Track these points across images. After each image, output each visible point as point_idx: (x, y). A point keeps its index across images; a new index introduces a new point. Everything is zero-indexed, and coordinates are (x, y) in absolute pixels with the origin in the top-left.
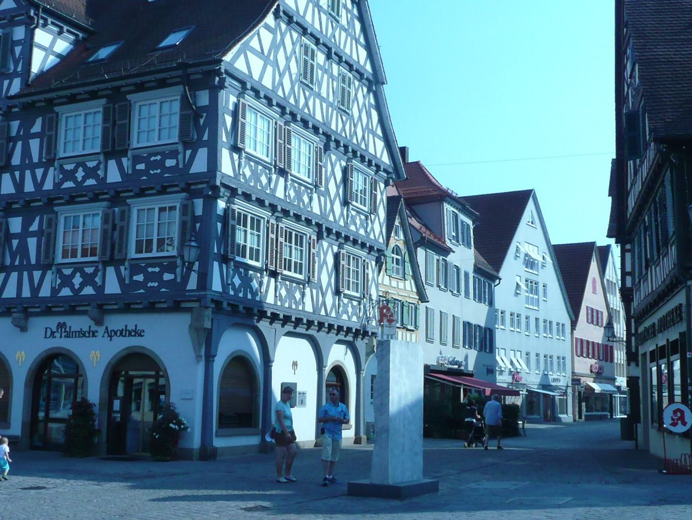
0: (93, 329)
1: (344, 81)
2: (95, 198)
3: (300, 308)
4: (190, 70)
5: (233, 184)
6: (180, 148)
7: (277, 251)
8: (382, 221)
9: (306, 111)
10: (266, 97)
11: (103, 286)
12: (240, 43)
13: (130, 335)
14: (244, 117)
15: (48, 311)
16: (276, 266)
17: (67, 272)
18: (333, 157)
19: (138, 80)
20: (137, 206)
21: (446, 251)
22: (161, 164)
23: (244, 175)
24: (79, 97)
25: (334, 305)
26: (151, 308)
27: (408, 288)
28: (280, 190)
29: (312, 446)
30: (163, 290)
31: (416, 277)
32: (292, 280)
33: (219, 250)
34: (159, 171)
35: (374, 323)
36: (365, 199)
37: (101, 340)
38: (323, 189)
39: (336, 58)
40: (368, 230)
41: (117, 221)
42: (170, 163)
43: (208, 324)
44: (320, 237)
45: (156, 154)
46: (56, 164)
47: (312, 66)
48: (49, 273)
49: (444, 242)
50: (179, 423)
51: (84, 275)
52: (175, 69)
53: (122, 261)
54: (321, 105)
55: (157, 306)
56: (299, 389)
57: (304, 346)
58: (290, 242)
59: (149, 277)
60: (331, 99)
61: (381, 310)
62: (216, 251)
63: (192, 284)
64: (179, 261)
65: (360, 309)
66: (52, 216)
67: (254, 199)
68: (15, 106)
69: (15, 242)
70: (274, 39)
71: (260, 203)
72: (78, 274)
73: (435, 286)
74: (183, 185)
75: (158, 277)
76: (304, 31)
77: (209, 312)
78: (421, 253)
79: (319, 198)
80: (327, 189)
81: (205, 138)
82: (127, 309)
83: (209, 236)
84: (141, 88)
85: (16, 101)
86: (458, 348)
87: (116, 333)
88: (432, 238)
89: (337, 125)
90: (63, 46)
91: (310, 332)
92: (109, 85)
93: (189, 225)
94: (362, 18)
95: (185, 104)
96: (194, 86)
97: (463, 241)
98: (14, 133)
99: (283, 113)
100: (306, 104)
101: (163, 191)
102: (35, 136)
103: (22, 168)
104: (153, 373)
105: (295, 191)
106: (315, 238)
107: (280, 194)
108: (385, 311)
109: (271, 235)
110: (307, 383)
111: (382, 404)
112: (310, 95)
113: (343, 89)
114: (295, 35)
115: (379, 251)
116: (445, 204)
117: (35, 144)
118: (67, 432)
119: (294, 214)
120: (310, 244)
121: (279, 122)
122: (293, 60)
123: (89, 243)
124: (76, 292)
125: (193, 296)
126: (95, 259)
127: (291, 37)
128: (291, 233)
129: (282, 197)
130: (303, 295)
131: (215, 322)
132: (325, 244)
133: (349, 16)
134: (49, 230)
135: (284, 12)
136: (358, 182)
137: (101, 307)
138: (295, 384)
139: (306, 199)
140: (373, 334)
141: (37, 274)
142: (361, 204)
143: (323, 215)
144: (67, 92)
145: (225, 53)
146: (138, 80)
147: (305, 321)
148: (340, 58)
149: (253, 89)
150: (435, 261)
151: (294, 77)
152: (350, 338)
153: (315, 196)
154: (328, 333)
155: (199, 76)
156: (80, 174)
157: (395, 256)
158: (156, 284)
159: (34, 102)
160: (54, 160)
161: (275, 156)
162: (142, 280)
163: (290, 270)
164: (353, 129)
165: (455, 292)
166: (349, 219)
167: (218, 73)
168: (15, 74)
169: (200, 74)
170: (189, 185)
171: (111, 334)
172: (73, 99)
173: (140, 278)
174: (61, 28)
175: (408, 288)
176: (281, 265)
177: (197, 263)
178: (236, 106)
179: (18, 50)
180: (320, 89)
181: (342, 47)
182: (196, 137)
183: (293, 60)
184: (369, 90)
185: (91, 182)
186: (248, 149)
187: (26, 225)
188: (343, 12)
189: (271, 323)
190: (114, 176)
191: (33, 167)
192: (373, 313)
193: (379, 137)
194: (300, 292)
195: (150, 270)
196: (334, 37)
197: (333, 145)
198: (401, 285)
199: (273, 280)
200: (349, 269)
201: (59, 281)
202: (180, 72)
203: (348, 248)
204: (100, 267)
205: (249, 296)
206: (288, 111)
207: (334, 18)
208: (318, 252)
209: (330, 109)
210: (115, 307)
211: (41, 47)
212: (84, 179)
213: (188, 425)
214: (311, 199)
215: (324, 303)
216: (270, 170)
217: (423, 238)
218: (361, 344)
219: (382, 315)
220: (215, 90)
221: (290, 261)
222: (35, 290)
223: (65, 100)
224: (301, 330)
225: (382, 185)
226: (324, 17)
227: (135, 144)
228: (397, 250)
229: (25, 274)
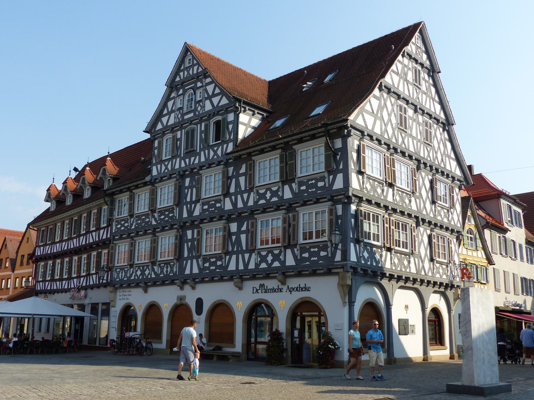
0: (281, 287)
1: (427, 125)
2: (278, 209)
3: (408, 270)
4: (329, 128)
5: (360, 194)
6: (326, 174)
7: (390, 235)
8: (458, 212)
9: (403, 146)
10: (377, 140)
11: (285, 261)
12: (359, 108)
13: (302, 290)
14: (364, 153)
15: (254, 277)
16: (390, 244)
17: (264, 253)
18: (423, 174)
19: (298, 136)
21: (505, 231)
22: (315, 185)
23: (366, 188)
24: (265, 150)
25: (430, 268)
26: (314, 273)
27: (480, 255)
28: (390, 196)
29: (421, 360)
30: (321, 262)
31: (485, 248)
32: (401, 253)
33: (353, 235)
34: (314, 190)
35: (458, 279)
36: (446, 199)
37: (285, 294)
38: (418, 194)
39: (421, 112)
40: (450, 219)
41: (291, 221)
42: (320, 184)
43: (349, 282)
44: (418, 225)
45: (312, 180)
46: (254, 190)
47: (405, 118)
48: (253, 254)
49: (503, 225)
50: (334, 344)
51: (273, 255)
52: (320, 127)
53: (295, 246)
54: (413, 142)
55: (318, 272)
56: (410, 323)
57: (412, 294)
58: (399, 229)
59: (312, 254)
60: (419, 137)
61: (462, 270)
62: (351, 236)
63: (338, 257)
64: (329, 244)
65: (448, 270)
66: (254, 221)
67: (373, 203)
68: (230, 159)
69: (234, 238)
70: (380, 104)
71: (378, 205)
72: (270, 255)
73: (499, 254)
74: (329, 197)
75: (317, 254)
76: (399, 97)
77: (349, 275)
78: (487, 232)
79: (415, 199)
80: (421, 194)
81: (341, 167)
82: (300, 274)
83: (347, 227)
84: (301, 141)
85: (231, 156)
86: (518, 295)
87: (293, 289)
88: (494, 222)
89: (424, 154)
90: (255, 122)
91: (415, 286)
92: (282, 141)
93: (334, 221)
94: (435, 85)
95: (328, 148)
96: (332, 137)
97: (516, 224)
98: (230, 174)
99: (389, 148)
100: (403, 142)
101: (317, 201)
102: (242, 175)
103: (236, 194)
104: (317, 313)
105: (400, 196)
106: (415, 226)
107: (390, 198)
108: (465, 271)
109: (386, 225)
110: (416, 319)
111: (466, 331)
112: (405, 136)
113: (427, 130)
114: (393, 100)
115: (458, 232)
116: (501, 200)
117: (242, 180)
118: (267, 350)
119: (400, 211)
120: (411, 229)
121: (386, 154)
122: (393, 116)
123: (275, 235)
124: (269, 265)
125: (339, 265)
126: (279, 245)
127: (390, 102)
128: (399, 223)
129: (391, 200)
130: (409, 262)
131: (353, 280)
132: (421, 229)
133: (427, 84)
134: (252, 229)
135: (385, 87)
136: (441, 189)
137: (285, 274)
138: (408, 320)
139: (407, 201)
140: (458, 286)
141: (247, 256)
142: (444, 202)
143: (419, 211)
144: (258, 148)
145: (350, 114)
146: (298, 136)
147: (411, 279)
148: (423, 111)
149: (368, 135)
150: (497, 237)
151: (394, 125)
152: (442, 289)
153: (413, 199)
154: (427, 286)
155: (335, 130)
156: (268, 195)
157: (469, 235)
158: (316, 259)
159: (241, 156)
160: (253, 188)
161: (386, 175)
163: (399, 246)
164: (435, 155)
165: (513, 258)
166: (437, 213)
167: (346, 127)
168: (230, 140)
169: (336, 129)
170: (332, 197)
171: (291, 290)
172: (262, 152)
173: (306, 255)
174: (254, 112)
175: (480, 255)
176: (393, 243)
177: (340, 245)
178: (359, 146)
179: (230, 127)
180: (411, 132)
181: (424, 104)
182: (335, 167)
183: (393, 116)
184: (444, 130)
185: (275, 199)
186: (368, 172)
187: (239, 227)
188: (423, 83)
189: (389, 281)
190: (288, 194)
191: (242, 193)
192: (458, 273)
193: (453, 159)
194: (407, 260)
195: (312, 250)
196: (418, 98)
197: (422, 166)
198: (475, 254)
199: (389, 253)
200: (438, 245)
201: (259, 259)
202: (323, 129)
203: (437, 231)
204: (283, 250)
205: (374, 264)
206: (392, 147)
207: (417, 87)
208: (418, 235)
209: (419, 144)
210: (293, 273)
211: (243, 124)
212: (271, 197)
213: (340, 346)
214: (410, 201)
215: (423, 267)
216: (383, 184)
217: (488, 223)
218: (450, 293)
219: (463, 274)
220: (345, 138)
221: (399, 241)
222: (246, 265)
223: (258, 152)
224: (409, 284)
225: (457, 190)
226: (411, 87)
227: (299, 175)
228: (470, 232)
229: (240, 255)
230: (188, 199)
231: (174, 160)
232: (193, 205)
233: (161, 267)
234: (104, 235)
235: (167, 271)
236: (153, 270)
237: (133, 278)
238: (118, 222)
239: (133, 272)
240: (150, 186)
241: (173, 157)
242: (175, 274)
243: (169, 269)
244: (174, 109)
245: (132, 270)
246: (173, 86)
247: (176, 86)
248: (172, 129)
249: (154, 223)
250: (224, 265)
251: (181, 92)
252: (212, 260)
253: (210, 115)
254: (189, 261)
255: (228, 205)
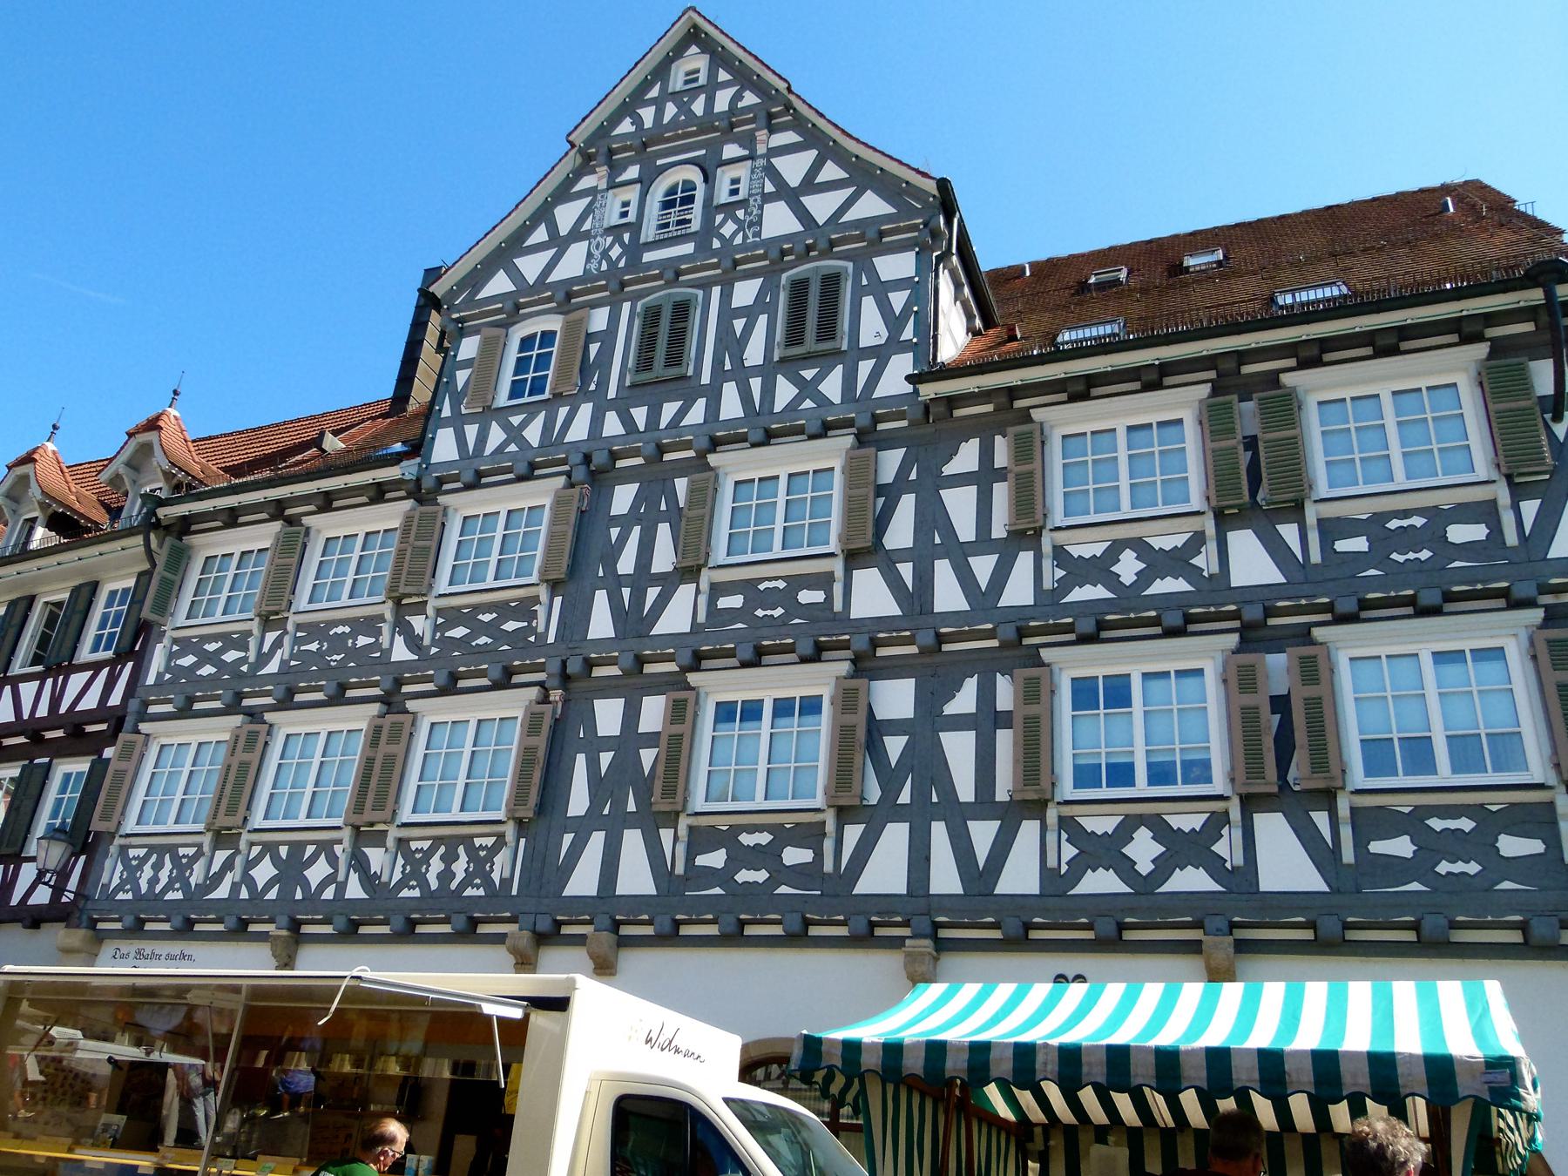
6: (1503, 494)
17: (1101, 824)
20: (1346, 645)
30: (1507, 885)
45: (1406, 514)
69: (895, 746)
141: (983, 834)
156: (1128, 567)
162: (1410, 855)
195: (1437, 824)
204: (1235, 814)
229: (939, 831)
230: (626, 564)
231: (563, 412)
232: (653, 593)
233: (409, 856)
234: (83, 692)
235: (446, 876)
236: (359, 863)
237: (222, 892)
238: (185, 646)
239: (228, 865)
240: (408, 504)
241: (558, 397)
242: (496, 894)
243: (460, 867)
244: (587, 226)
245: (221, 856)
246: (596, 151)
247: (611, 152)
248: (567, 298)
249: (401, 652)
250: (828, 866)
251: (633, 172)
252: (747, 839)
253: (783, 253)
254: (597, 840)
255: (871, 597)
